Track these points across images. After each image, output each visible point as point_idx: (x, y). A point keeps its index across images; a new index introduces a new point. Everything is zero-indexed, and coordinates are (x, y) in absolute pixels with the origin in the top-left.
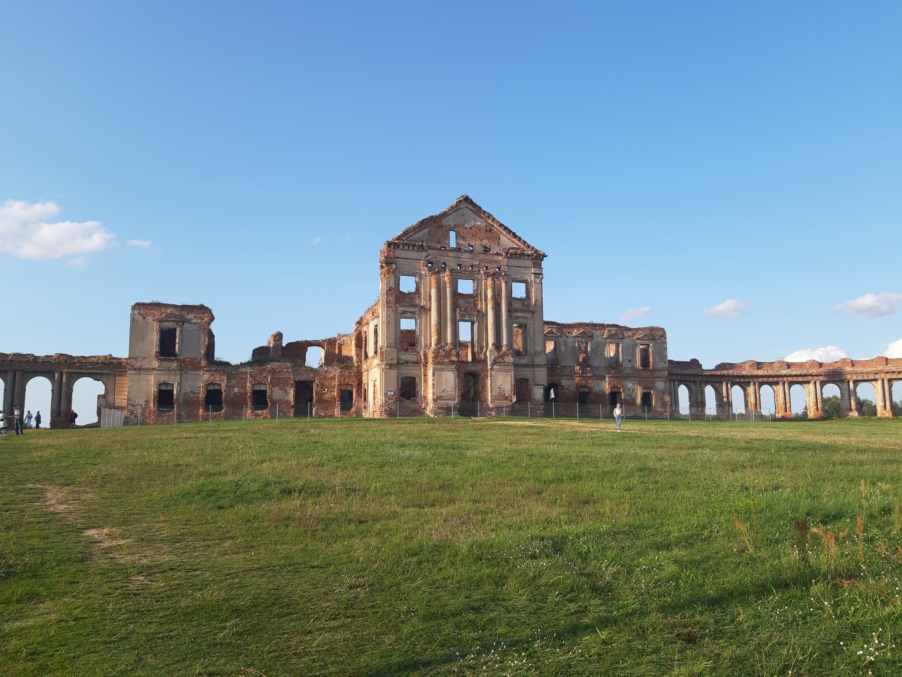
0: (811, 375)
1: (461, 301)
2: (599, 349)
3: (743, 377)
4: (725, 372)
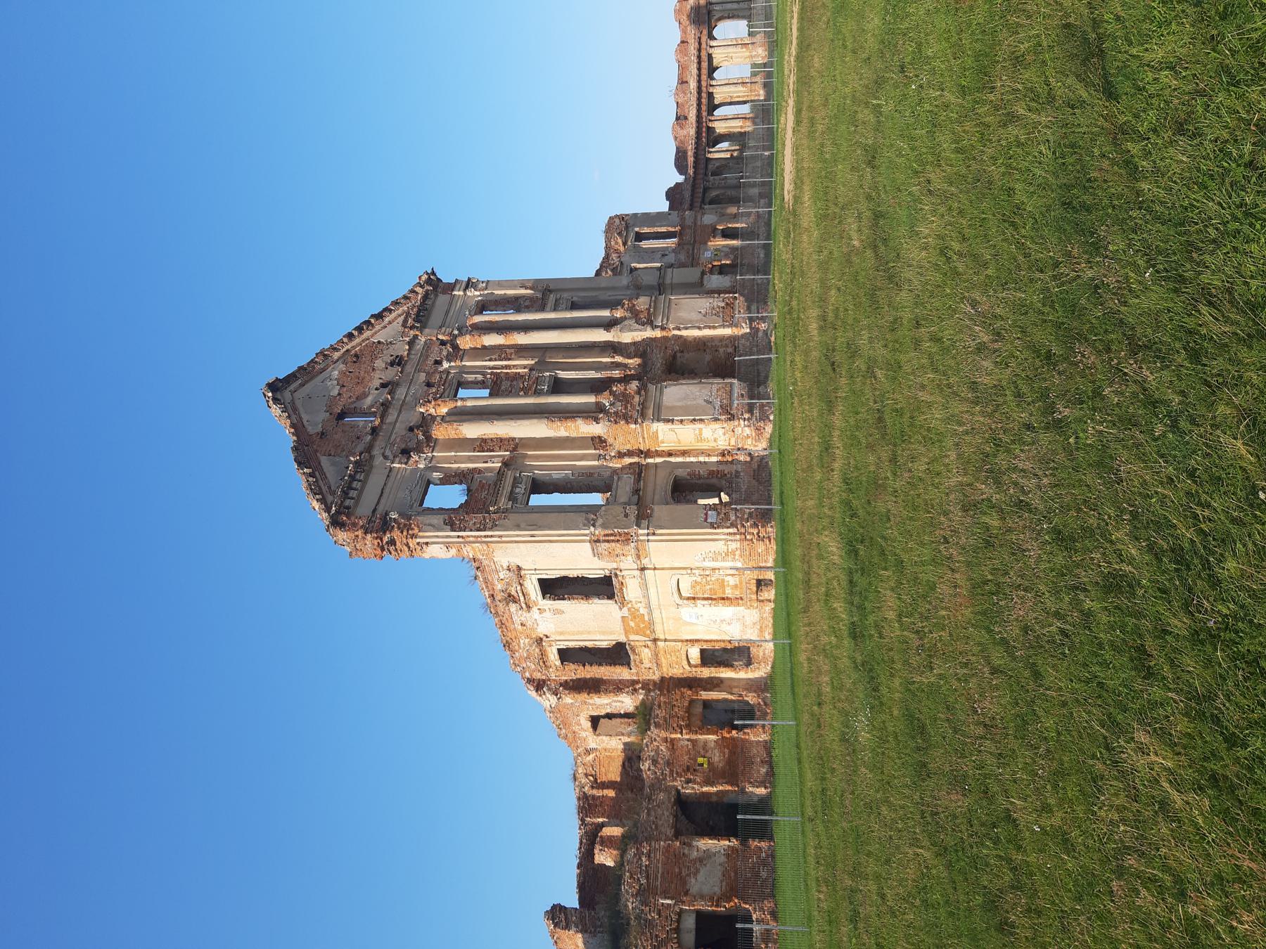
0: (699, 50)
4: (691, 159)
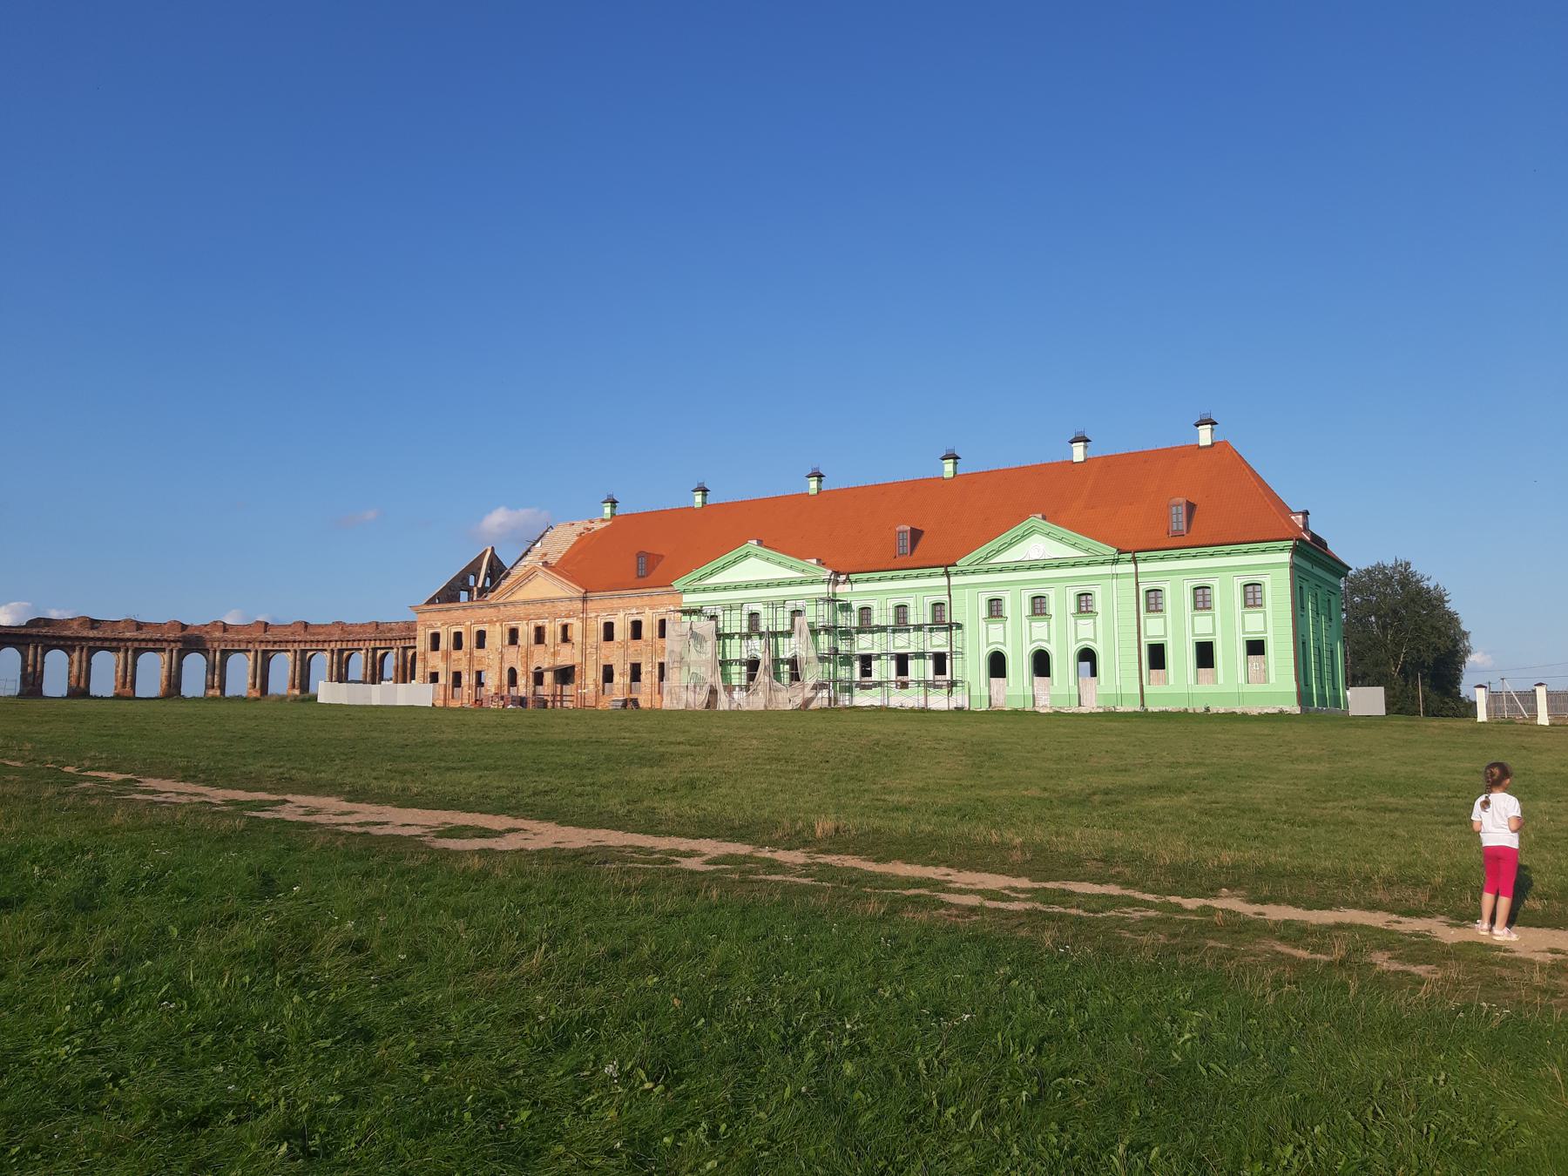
3: (69, 638)
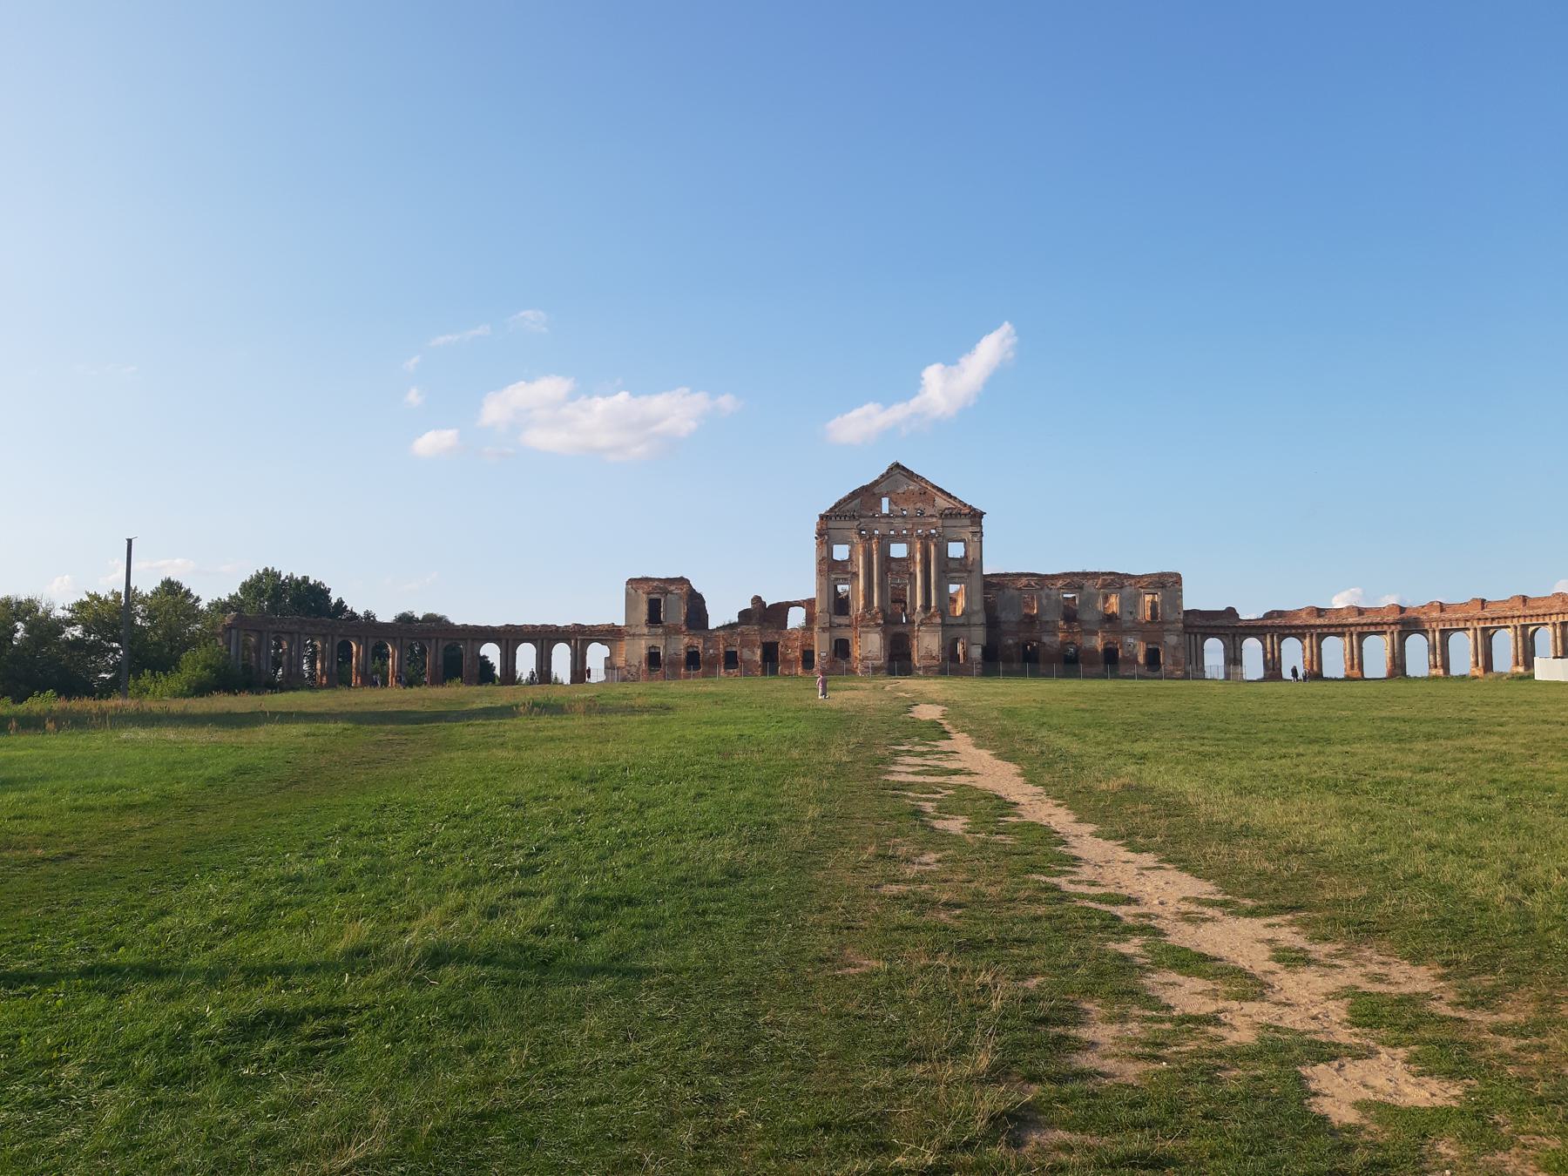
1: (893, 565)
2: (1089, 602)
